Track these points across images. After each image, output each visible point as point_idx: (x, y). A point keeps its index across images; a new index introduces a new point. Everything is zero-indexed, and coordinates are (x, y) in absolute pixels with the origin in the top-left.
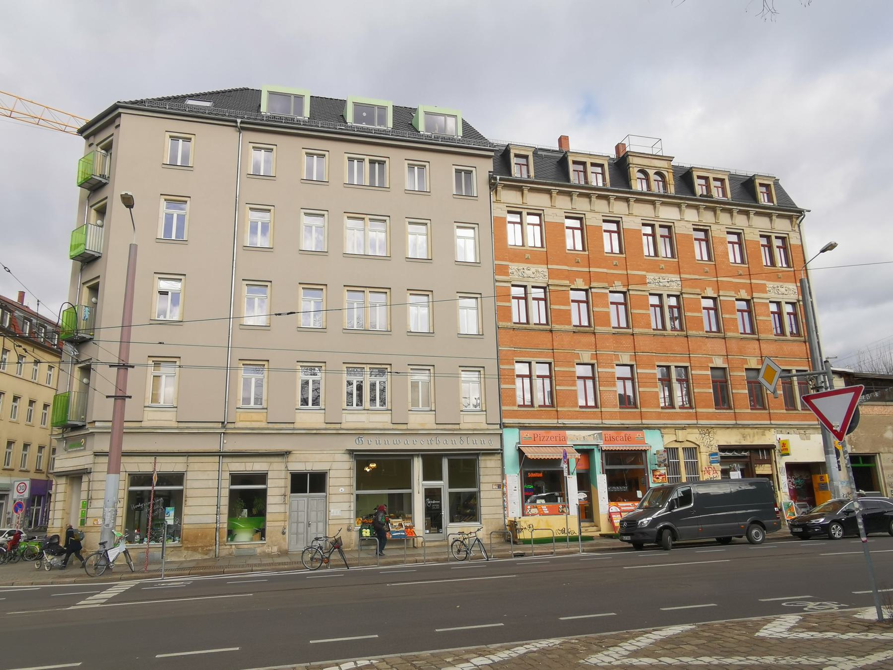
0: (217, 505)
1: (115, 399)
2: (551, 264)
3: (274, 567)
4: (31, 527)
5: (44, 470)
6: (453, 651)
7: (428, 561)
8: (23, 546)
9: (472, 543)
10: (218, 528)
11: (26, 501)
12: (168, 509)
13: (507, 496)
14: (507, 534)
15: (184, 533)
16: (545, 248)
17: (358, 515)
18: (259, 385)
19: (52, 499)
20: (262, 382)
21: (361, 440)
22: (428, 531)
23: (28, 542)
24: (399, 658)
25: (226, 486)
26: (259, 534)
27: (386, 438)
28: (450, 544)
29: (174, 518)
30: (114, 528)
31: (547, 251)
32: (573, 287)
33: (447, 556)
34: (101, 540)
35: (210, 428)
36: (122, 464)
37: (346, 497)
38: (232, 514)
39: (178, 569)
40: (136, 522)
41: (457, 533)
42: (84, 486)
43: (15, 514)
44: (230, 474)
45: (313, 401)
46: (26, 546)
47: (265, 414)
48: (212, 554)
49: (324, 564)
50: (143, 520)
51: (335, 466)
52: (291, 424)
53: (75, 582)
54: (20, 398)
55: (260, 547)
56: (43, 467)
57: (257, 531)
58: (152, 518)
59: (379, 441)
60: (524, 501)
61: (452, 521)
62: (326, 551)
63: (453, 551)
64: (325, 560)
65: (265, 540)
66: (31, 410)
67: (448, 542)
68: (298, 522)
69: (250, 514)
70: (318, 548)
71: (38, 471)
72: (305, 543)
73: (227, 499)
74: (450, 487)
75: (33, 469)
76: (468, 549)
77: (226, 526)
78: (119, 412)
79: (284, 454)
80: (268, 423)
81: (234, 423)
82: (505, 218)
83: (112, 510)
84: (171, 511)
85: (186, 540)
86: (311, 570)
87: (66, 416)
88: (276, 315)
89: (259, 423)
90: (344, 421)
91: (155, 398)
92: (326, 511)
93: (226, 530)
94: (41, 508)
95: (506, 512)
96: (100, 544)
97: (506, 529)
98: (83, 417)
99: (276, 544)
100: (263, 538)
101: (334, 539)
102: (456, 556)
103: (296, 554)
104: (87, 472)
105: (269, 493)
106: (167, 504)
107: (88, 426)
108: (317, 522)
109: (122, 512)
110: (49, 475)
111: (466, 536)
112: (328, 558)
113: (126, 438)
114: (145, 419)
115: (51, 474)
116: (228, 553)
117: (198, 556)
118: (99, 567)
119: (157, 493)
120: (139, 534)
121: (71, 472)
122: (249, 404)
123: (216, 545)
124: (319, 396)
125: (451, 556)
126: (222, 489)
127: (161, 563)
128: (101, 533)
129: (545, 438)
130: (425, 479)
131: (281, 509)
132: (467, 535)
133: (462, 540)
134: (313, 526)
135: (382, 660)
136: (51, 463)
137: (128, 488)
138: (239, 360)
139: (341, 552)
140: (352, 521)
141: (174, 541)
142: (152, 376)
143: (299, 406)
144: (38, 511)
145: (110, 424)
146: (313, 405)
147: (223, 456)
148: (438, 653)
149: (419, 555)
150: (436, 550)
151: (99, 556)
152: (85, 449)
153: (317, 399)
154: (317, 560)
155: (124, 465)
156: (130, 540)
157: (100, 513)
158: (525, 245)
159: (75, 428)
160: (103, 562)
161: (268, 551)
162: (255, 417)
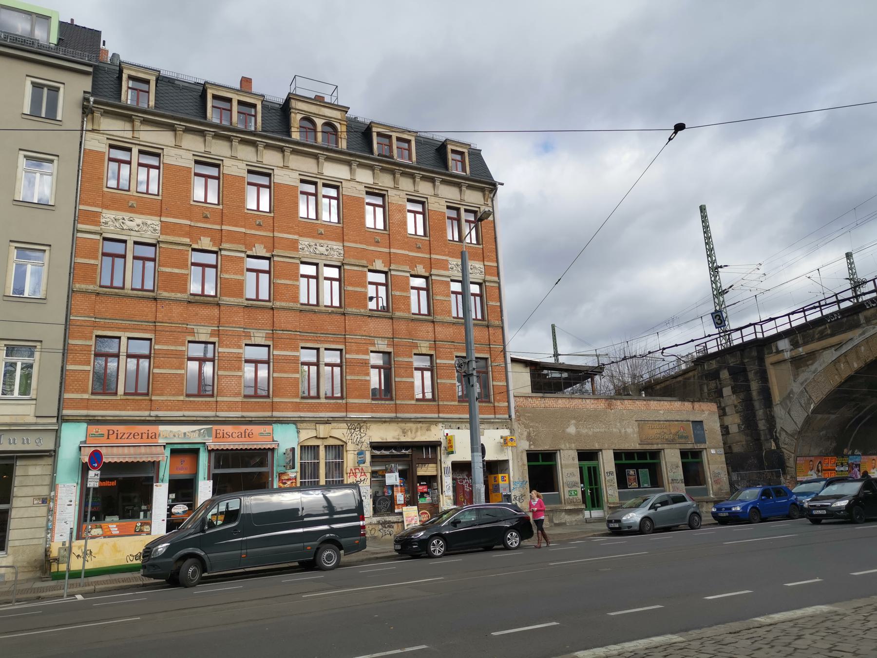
129: (126, 436)
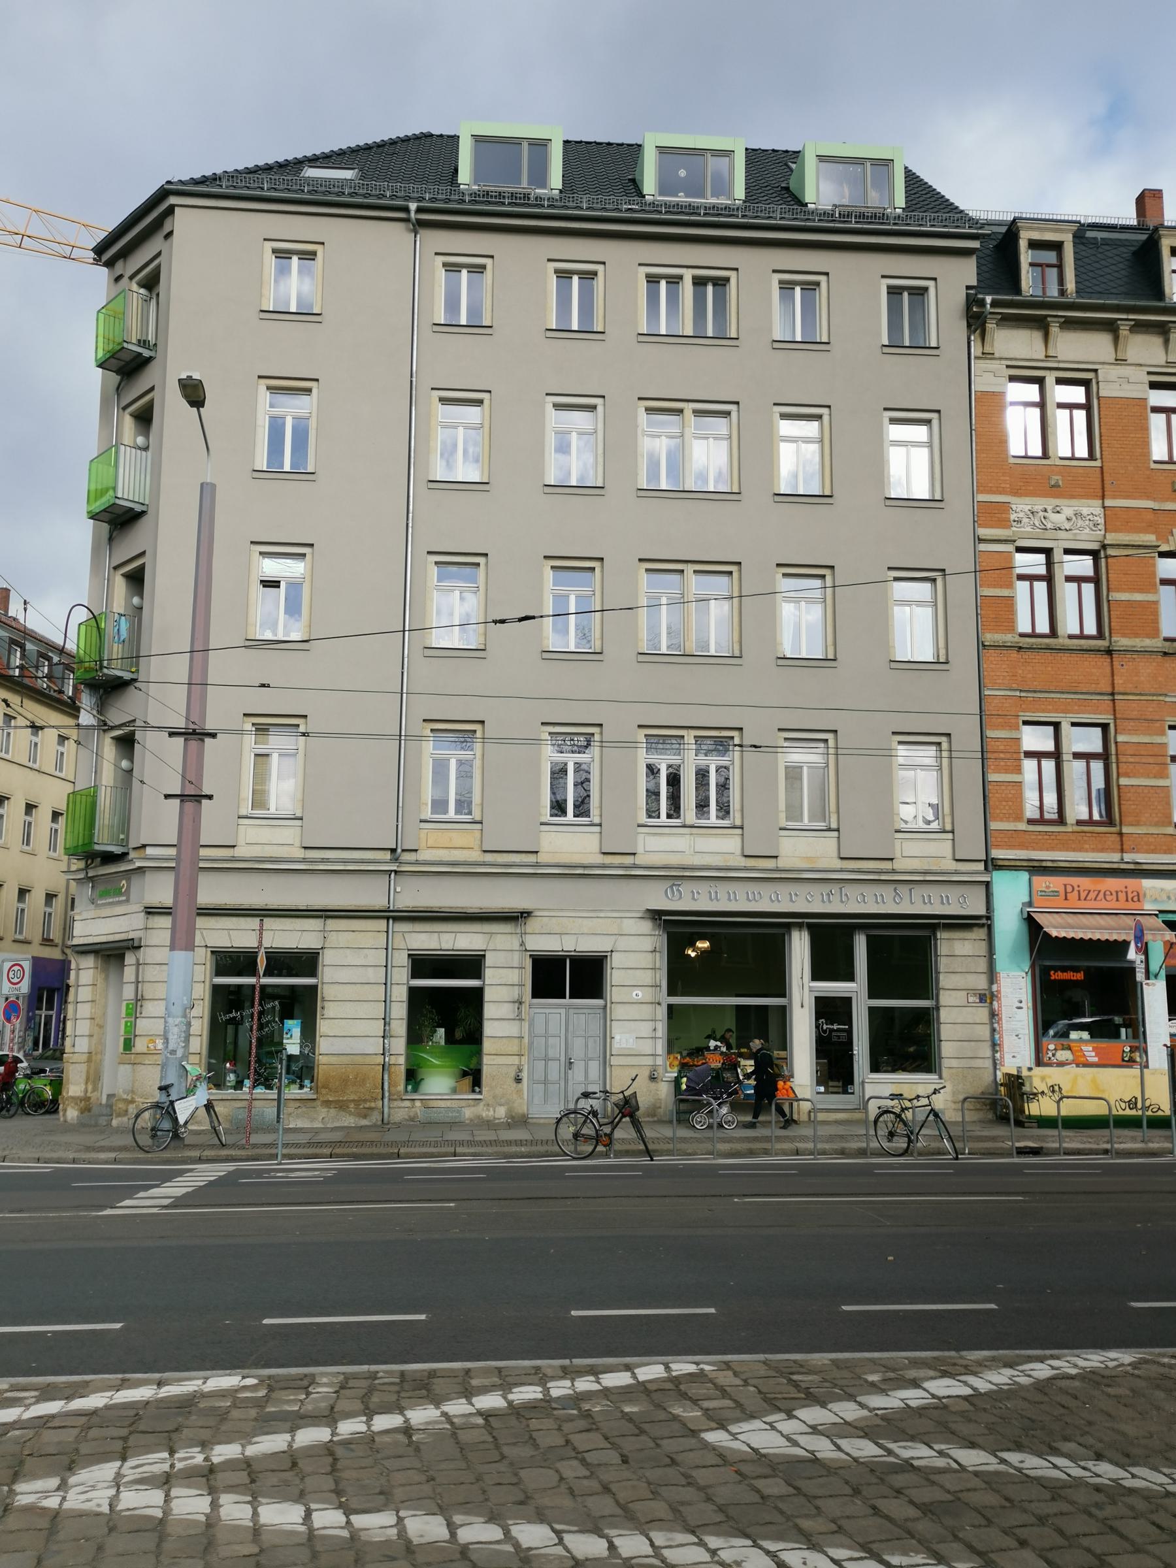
0: (384, 1019)
1: (182, 801)
2: (1114, 497)
3: (499, 1149)
4: (38, 1050)
5: (58, 939)
6: (881, 1359)
7: (823, 1152)
8: (22, 1086)
9: (921, 1117)
10: (387, 1064)
11: (26, 999)
12: (289, 1023)
13: (1000, 1019)
14: (1000, 1103)
15: (321, 1072)
16: (1099, 461)
17: (671, 1047)
18: (465, 773)
19: (71, 998)
20: (471, 766)
21: (678, 890)
22: (822, 1089)
23: (30, 1078)
24: (762, 1364)
25: (402, 980)
26: (468, 1081)
27: (731, 887)
28: (872, 1117)
29: (301, 1042)
30: (185, 1057)
31: (1102, 467)
32: (1164, 548)
33: (864, 1145)
34: (161, 1080)
35: (363, 862)
36: (198, 933)
37: (646, 1011)
38: (415, 1037)
39: (310, 1144)
40: (230, 1047)
41: (888, 1095)
42: (129, 973)
43: (8, 1025)
44: (409, 955)
45: (575, 806)
46: (28, 1087)
47: (478, 834)
48: (375, 1118)
49: (600, 1148)
50: (243, 1043)
51: (623, 943)
52: (530, 855)
53: (115, 1161)
54: (8, 798)
55: (471, 1108)
56: (55, 934)
57: (465, 1074)
58: (259, 1040)
59: (716, 892)
60: (1040, 1031)
61: (875, 1068)
62: (606, 1120)
63: (880, 1133)
64: (603, 1140)
65: (480, 1093)
66: (30, 824)
67: (867, 1113)
68: (546, 1059)
69: (450, 1039)
70: (589, 1114)
71: (47, 941)
72: (562, 1102)
73: (405, 1006)
74: (872, 995)
75: (37, 938)
76: (912, 1133)
77: (402, 1060)
78: (189, 829)
79: (518, 917)
80: (485, 851)
81: (416, 850)
82: (1001, 395)
83: (182, 1022)
84: (294, 1028)
85: (324, 1087)
86: (574, 1159)
87: (92, 836)
88: (495, 622)
89: (465, 852)
90: (640, 850)
91: (259, 799)
92: (605, 1038)
93: (403, 1069)
94: (53, 1013)
95: (998, 1055)
96: (161, 1089)
97: (997, 1092)
98: (122, 836)
99: (503, 1101)
100: (477, 1089)
101: (621, 1096)
102: (886, 1145)
103: (544, 1124)
104: (133, 946)
105: (488, 995)
106: (287, 1014)
107: (132, 855)
108: (587, 1060)
109: (200, 1026)
110: (68, 951)
111: (908, 1104)
112: (609, 1136)
113: (204, 880)
114: (241, 841)
115: (68, 947)
116: (407, 1117)
117: (349, 1121)
118: (159, 1133)
119: (269, 990)
120: (235, 1072)
121: (104, 946)
122: (446, 812)
123: (382, 1099)
124: (589, 796)
125: (874, 1144)
126: (394, 986)
127: (276, 1131)
128: (163, 1068)
130: (816, 976)
131: (512, 1029)
132: (910, 1100)
133: (897, 1110)
134: (579, 1067)
135: (724, 1367)
136: (67, 927)
137: (211, 980)
138: (424, 720)
139: (636, 1124)
140: (659, 1061)
141: (302, 1087)
142: (253, 756)
143: (547, 818)
144: (48, 1019)
145: (172, 852)
146: (574, 816)
147: (395, 919)
148: (847, 1360)
149: (804, 1139)
150: (840, 1130)
151: (159, 1111)
152: (128, 901)
153: (583, 802)
154: (587, 1138)
155: (202, 933)
156: (217, 1082)
157: (157, 1027)
158: (1051, 453)
159: (109, 858)
160: (166, 1125)
161: (487, 1116)
162: (458, 839)
